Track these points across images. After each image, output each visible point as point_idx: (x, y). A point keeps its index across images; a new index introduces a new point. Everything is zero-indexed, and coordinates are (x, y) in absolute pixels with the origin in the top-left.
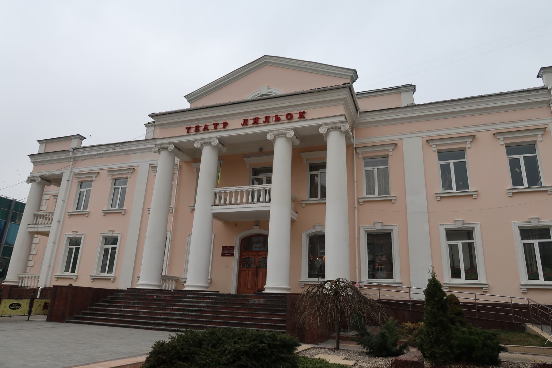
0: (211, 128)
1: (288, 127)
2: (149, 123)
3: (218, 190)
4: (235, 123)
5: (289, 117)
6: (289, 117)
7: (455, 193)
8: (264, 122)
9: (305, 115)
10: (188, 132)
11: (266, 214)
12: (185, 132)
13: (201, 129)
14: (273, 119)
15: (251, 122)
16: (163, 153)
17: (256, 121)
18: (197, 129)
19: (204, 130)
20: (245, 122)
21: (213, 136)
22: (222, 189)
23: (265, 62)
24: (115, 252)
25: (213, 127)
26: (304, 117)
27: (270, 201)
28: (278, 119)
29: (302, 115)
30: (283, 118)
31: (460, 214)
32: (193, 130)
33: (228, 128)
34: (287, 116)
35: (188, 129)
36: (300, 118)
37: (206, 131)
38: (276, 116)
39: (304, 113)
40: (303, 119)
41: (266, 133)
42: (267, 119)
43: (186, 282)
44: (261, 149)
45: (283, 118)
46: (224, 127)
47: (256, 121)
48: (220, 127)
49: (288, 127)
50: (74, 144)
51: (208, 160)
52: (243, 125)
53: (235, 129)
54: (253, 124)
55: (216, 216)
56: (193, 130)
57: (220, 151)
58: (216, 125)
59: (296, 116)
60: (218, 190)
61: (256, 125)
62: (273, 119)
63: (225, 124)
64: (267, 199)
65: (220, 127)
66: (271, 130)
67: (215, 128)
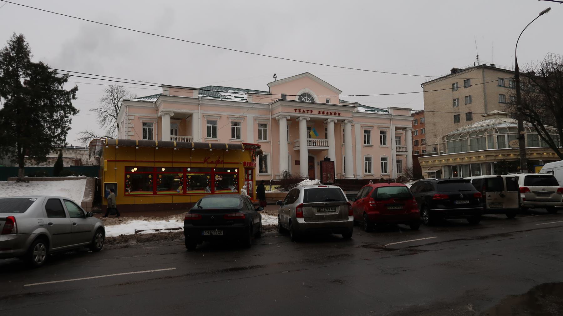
0: (306, 111)
1: (336, 118)
4: (315, 112)
6: (335, 114)
12: (294, 111)
13: (302, 111)
15: (321, 113)
17: (323, 113)
18: (300, 111)
20: (319, 112)
23: (306, 75)
28: (331, 114)
29: (339, 114)
31: (369, 152)
32: (297, 111)
35: (296, 110)
42: (328, 113)
47: (323, 113)
48: (309, 112)
49: (336, 118)
51: (303, 126)
53: (315, 115)
56: (297, 111)
58: (308, 111)
63: (312, 111)
65: (309, 112)
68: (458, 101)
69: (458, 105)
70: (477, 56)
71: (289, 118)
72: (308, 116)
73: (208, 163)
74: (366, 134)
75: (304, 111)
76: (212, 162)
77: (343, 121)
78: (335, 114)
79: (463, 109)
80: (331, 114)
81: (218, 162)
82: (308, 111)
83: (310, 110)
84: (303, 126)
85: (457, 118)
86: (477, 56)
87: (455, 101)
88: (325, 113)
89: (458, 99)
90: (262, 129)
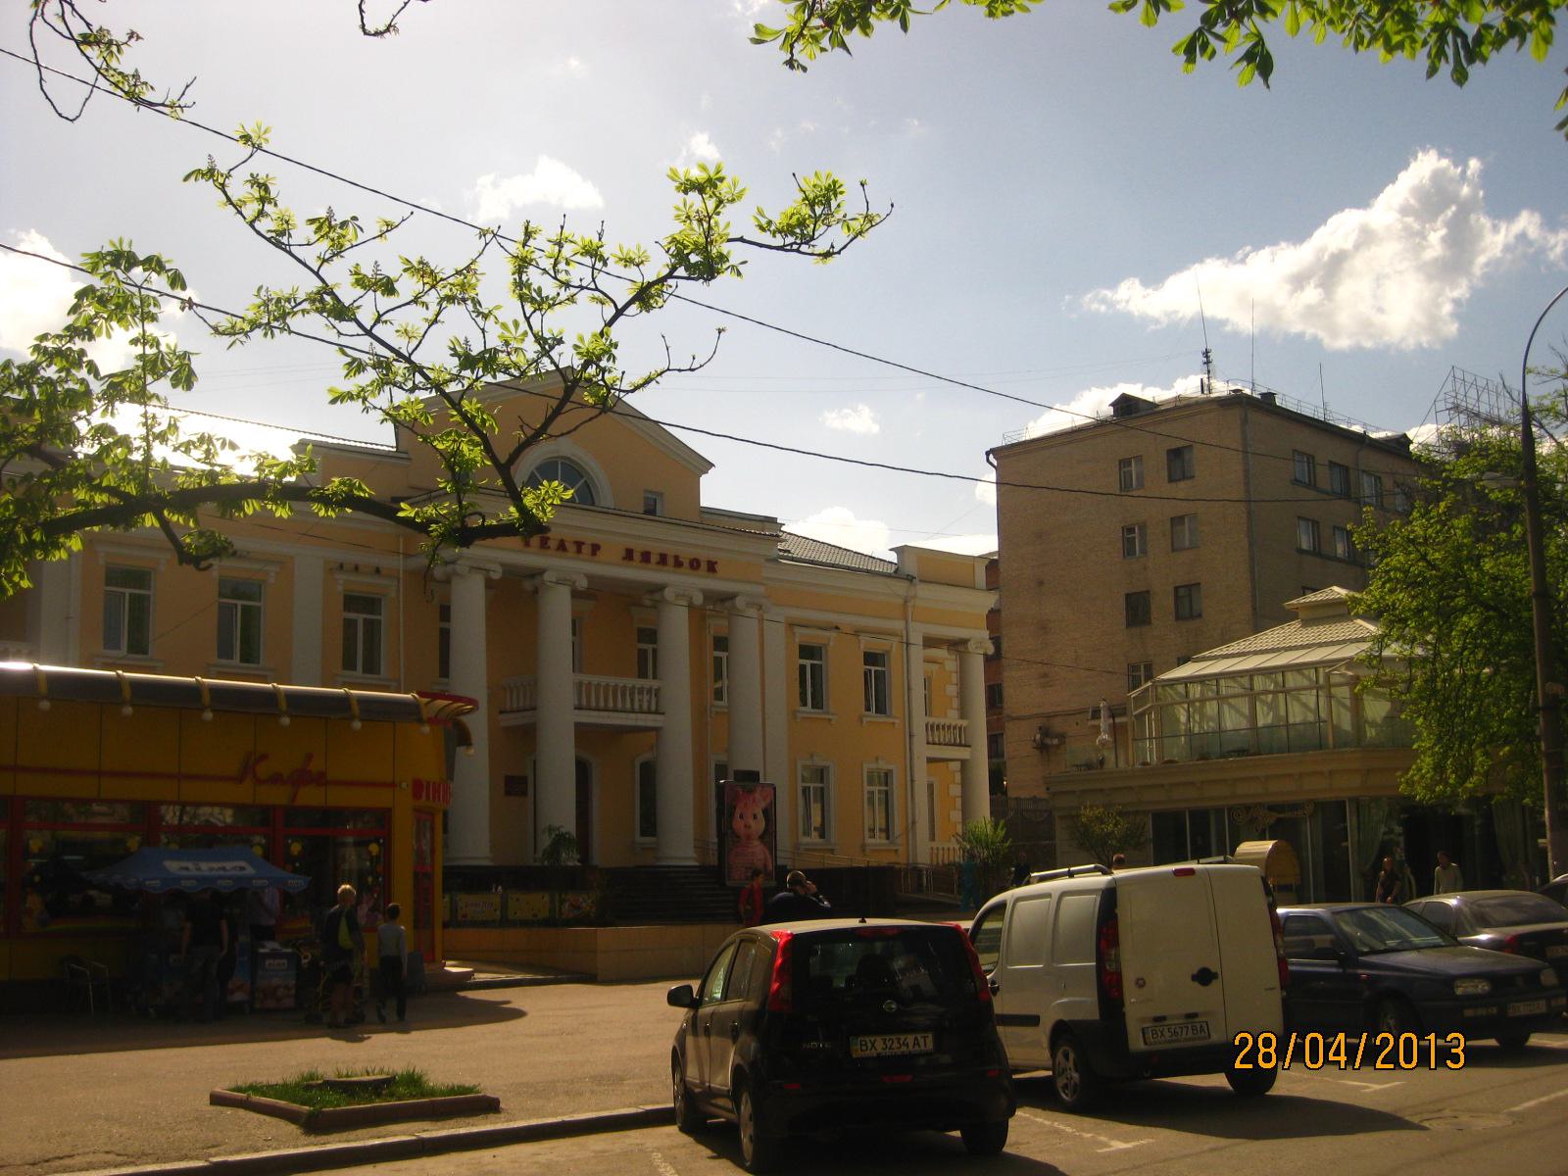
0: (571, 548)
1: (697, 584)
6: (695, 564)
7: (810, 713)
8: (658, 563)
19: (558, 549)
20: (629, 555)
28: (678, 564)
29: (712, 567)
30: (686, 564)
33: (601, 555)
38: (676, 558)
39: (716, 563)
49: (697, 584)
52: (624, 558)
61: (644, 565)
63: (596, 548)
65: (586, 549)
67: (579, 551)
68: (1143, 535)
69: (1144, 552)
70: (1206, 354)
71: (583, 584)
72: (580, 569)
73: (259, 781)
74: (808, 663)
76: (276, 779)
77: (728, 598)
78: (695, 564)
79: (1161, 573)
80: (678, 564)
81: (303, 777)
82: (579, 545)
83: (590, 538)
84: (558, 610)
85: (1137, 610)
86: (1206, 354)
87: (1131, 539)
88: (654, 558)
89: (1143, 527)
90: (360, 618)
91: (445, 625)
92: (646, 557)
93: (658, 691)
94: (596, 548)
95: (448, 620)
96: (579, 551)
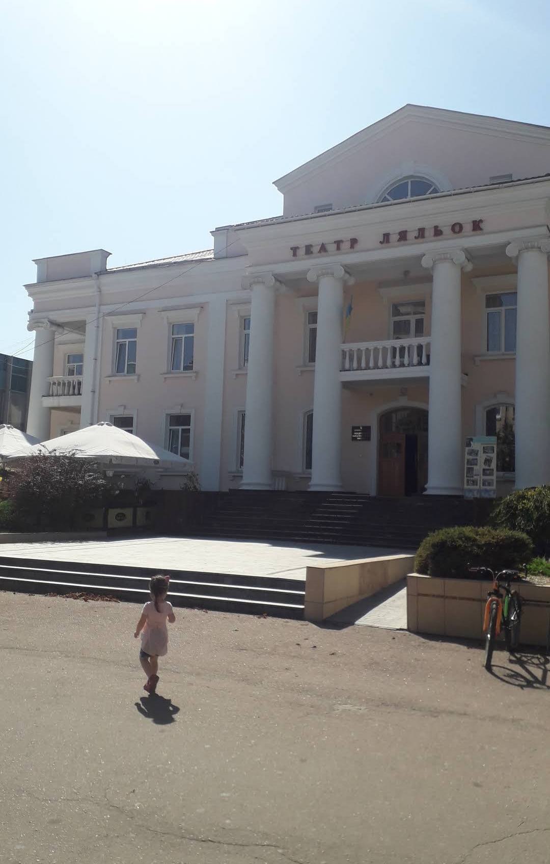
0: (332, 248)
2: (218, 230)
3: (347, 347)
5: (457, 229)
9: (482, 225)
10: (295, 255)
11: (424, 382)
13: (316, 249)
14: (429, 233)
15: (394, 238)
16: (258, 288)
19: (320, 252)
20: (386, 238)
21: (337, 261)
22: (354, 346)
24: (189, 437)
25: (335, 245)
26: (481, 229)
27: (428, 363)
28: (438, 232)
30: (447, 231)
32: (302, 252)
33: (358, 247)
34: (453, 227)
35: (295, 250)
36: (474, 230)
37: (323, 253)
38: (436, 228)
39: (481, 221)
40: (479, 232)
41: (420, 257)
43: (310, 478)
44: (406, 273)
45: (447, 231)
46: (352, 247)
48: (346, 246)
50: (96, 266)
54: (399, 240)
55: (346, 385)
56: (302, 252)
57: (345, 283)
59: (468, 227)
60: (347, 347)
61: (402, 242)
62: (429, 233)
63: (354, 242)
64: (424, 360)
65: (346, 246)
66: (428, 248)
67: (338, 248)
72: (337, 261)
75: (323, 248)
78: (457, 228)
80: (438, 232)
82: (338, 243)
83: (346, 236)
91: (312, 326)
92: (403, 236)
93: (428, 345)
94: (354, 242)
95: (315, 322)
96: (338, 248)
